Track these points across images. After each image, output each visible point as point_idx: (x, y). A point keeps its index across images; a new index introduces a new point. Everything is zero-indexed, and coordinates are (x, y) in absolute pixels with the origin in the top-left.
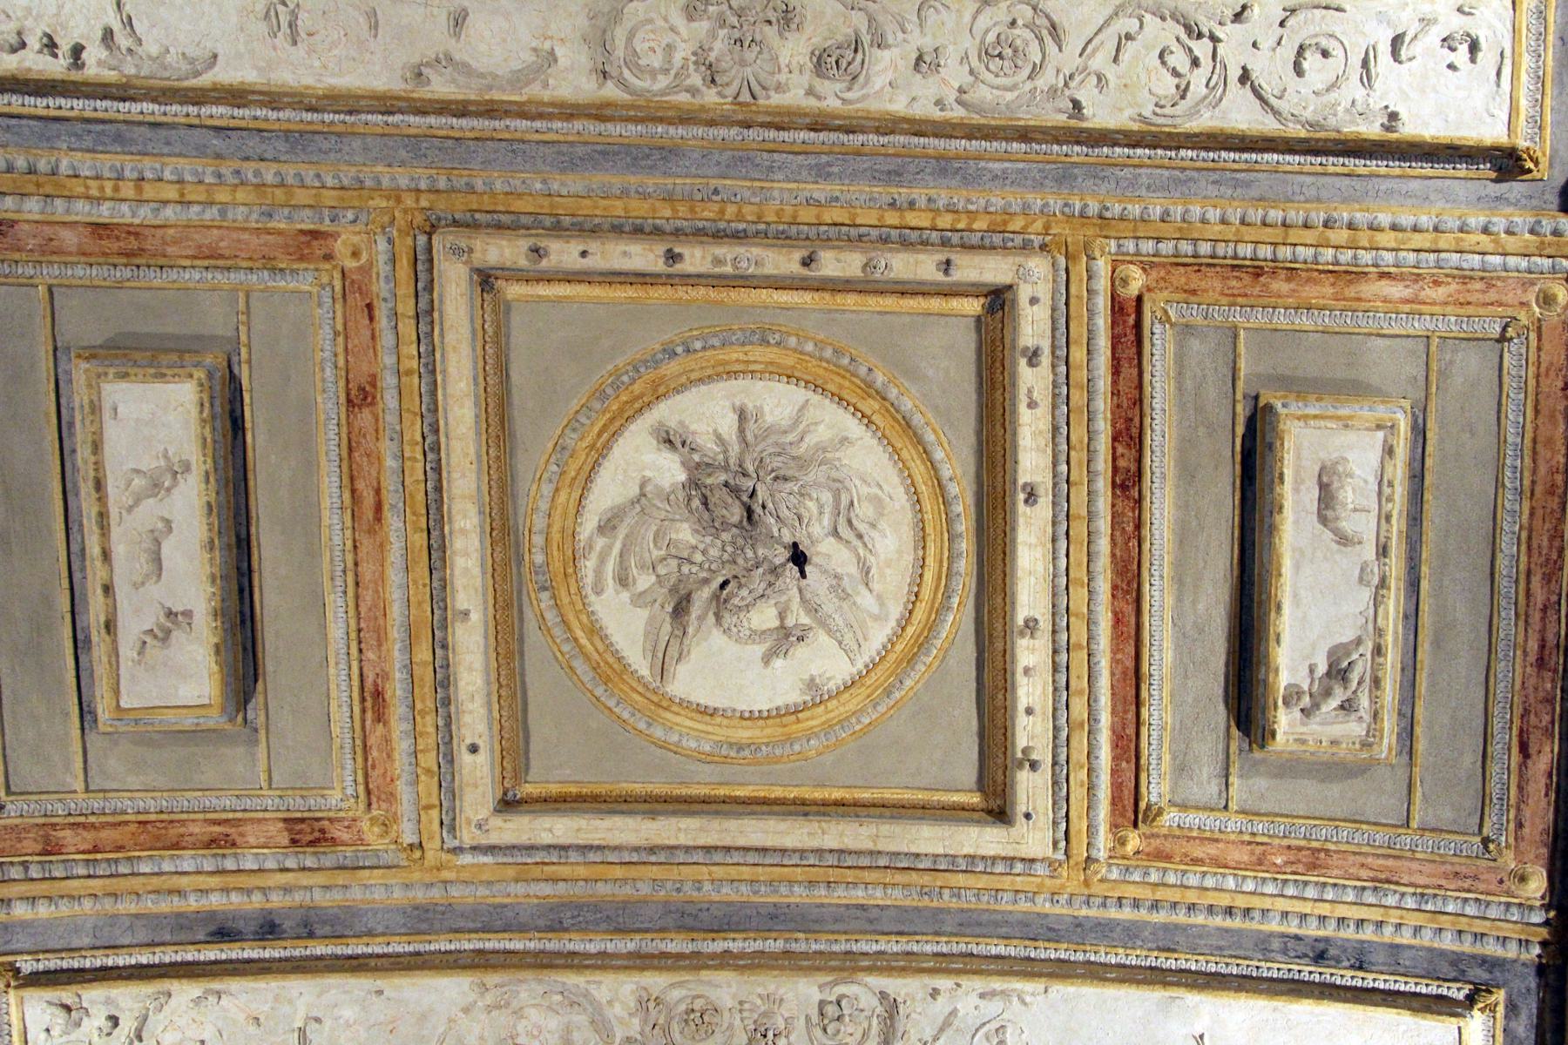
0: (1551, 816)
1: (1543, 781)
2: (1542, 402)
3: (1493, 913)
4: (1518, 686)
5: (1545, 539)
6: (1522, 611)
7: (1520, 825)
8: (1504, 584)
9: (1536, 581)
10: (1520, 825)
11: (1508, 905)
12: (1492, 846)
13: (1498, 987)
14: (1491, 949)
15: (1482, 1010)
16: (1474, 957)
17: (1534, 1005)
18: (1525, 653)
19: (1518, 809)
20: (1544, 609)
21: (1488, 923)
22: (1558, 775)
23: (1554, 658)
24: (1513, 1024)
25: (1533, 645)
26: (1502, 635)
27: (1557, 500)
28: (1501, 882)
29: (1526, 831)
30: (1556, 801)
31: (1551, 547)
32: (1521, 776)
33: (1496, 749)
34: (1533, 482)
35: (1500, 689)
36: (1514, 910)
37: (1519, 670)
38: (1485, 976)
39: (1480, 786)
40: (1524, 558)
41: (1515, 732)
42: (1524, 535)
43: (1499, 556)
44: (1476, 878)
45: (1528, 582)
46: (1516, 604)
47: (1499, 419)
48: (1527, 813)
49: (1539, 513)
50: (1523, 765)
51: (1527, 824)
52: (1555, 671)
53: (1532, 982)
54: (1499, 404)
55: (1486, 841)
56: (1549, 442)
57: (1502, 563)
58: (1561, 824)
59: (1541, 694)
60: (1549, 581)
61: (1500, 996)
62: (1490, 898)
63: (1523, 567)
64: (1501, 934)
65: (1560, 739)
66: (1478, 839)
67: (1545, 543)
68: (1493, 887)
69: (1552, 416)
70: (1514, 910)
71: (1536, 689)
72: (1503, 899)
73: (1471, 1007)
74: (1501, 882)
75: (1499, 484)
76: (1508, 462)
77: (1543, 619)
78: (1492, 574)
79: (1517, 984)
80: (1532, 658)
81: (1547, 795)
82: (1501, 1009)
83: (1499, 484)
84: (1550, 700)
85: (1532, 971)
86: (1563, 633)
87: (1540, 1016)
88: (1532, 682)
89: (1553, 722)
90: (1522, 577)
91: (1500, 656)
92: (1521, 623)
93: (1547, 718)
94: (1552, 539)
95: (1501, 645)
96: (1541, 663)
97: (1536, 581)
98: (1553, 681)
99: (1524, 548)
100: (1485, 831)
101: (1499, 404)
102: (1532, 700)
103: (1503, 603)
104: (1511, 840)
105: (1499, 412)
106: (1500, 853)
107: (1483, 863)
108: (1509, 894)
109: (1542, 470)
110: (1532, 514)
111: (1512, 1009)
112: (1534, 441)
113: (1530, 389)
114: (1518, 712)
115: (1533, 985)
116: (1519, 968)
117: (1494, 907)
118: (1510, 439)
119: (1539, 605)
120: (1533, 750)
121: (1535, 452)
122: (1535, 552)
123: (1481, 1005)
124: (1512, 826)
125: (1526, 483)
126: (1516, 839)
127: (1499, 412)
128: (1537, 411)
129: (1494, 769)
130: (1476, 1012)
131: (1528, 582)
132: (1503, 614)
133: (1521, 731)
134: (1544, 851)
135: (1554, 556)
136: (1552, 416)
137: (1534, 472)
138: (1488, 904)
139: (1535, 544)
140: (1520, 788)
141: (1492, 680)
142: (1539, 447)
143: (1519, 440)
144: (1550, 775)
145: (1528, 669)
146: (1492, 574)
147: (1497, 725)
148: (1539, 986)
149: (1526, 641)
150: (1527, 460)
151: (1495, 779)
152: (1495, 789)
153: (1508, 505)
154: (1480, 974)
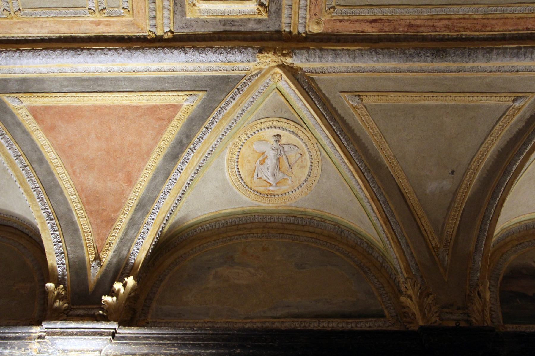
0: (345, 33)
1: (360, 29)
2: (523, 20)
3: (302, 12)
4: (402, 17)
5: (464, 25)
6: (434, 17)
7: (340, 21)
8: (446, 9)
9: (446, 22)
10: (340, 21)
11: (306, 18)
12: (332, 10)
13: (268, 16)
14: (285, 12)
15: (258, 9)
16: (281, 5)
17: (262, 30)
18: (416, 19)
19: (348, 20)
20: (434, 26)
21: (297, 10)
22: (363, 35)
23: (412, 31)
24: (252, 22)
25: (418, 22)
26: (424, 10)
27: (480, 28)
28: (315, 15)
29: (338, 24)
30: (351, 35)
31: (460, 27)
32: (362, 20)
33: (375, 10)
34: (488, 19)
35: (400, 10)
36: (304, 20)
37: (410, 17)
38: (272, 10)
39: (358, 4)
40: (457, 17)
41: (382, 17)
42: (467, 16)
43: (459, 7)
44: (316, 4)
45: (445, 19)
46: (437, 15)
47: (518, 3)
48: (347, 24)
49: (475, 22)
50: (367, 21)
51: (341, 24)
52: (407, 32)
53: (272, 29)
54: (524, 3)
55: (334, 7)
56: (505, 24)
57: (455, 8)
58: (343, 37)
59: (397, 27)
60: (445, 27)
61: (265, 16)
62: (308, 10)
63: (453, 16)
64: (292, 16)
65: (378, 35)
66: (334, 5)
67: (462, 25)
68: (313, 12)
69: (517, 24)
70: (304, 20)
71: (400, 25)
72: (308, 16)
73: (259, 5)
74: (315, 15)
75: (489, 5)
76: (499, 8)
77: (430, 26)
78: (450, 4)
79: (271, 23)
80: (413, 22)
81: (354, 31)
82: (259, 17)
83: (489, 5)
84: (395, 30)
85: (277, 28)
86: (423, 34)
87: (257, 32)
88: (403, 23)
89: (385, 32)
90: (449, 17)
91: (415, 10)
92: (429, 17)
93: (387, 29)
94: (464, 27)
95: (420, 10)
96: (411, 26)
97: (446, 22)
98: (403, 31)
99: (462, 16)
100: (338, 7)
101: (524, 3)
102: (395, 23)
103: (438, 10)
104: (334, 18)
105: (521, 3)
106: (329, 13)
107: (323, 7)
108: (310, 18)
109: (494, 22)
110: (475, 19)
111: (259, 21)
112: (507, 18)
113: (530, 15)
114: (391, 18)
115: (271, 29)
116: (277, 24)
117: (305, 12)
118: (509, 8)
119: (435, 24)
120: (373, 24)
121: (501, 19)
122: (458, 21)
123: (260, 8)
124: (341, 18)
125: (490, 16)
126: (335, 20)
127: (521, 3)
128: (519, 18)
129: (366, 10)
130: (258, 6)
131: (445, 19)
132: (433, 10)
133: (382, 20)
134: (330, 31)
135: (456, 29)
136: (517, 24)
137: (493, 19)
138: (306, 10)
139: (461, 21)
140: (357, 21)
141: (404, 7)
142: (503, 20)
143: (508, 12)
144: (362, 32)
145: (408, 21)
146: (450, 4)
147: (385, 10)
148: (271, 31)
149: (421, 20)
150: (499, 16)
151: (361, 10)
152: (357, 10)
153: (481, 9)
154: (273, 8)
